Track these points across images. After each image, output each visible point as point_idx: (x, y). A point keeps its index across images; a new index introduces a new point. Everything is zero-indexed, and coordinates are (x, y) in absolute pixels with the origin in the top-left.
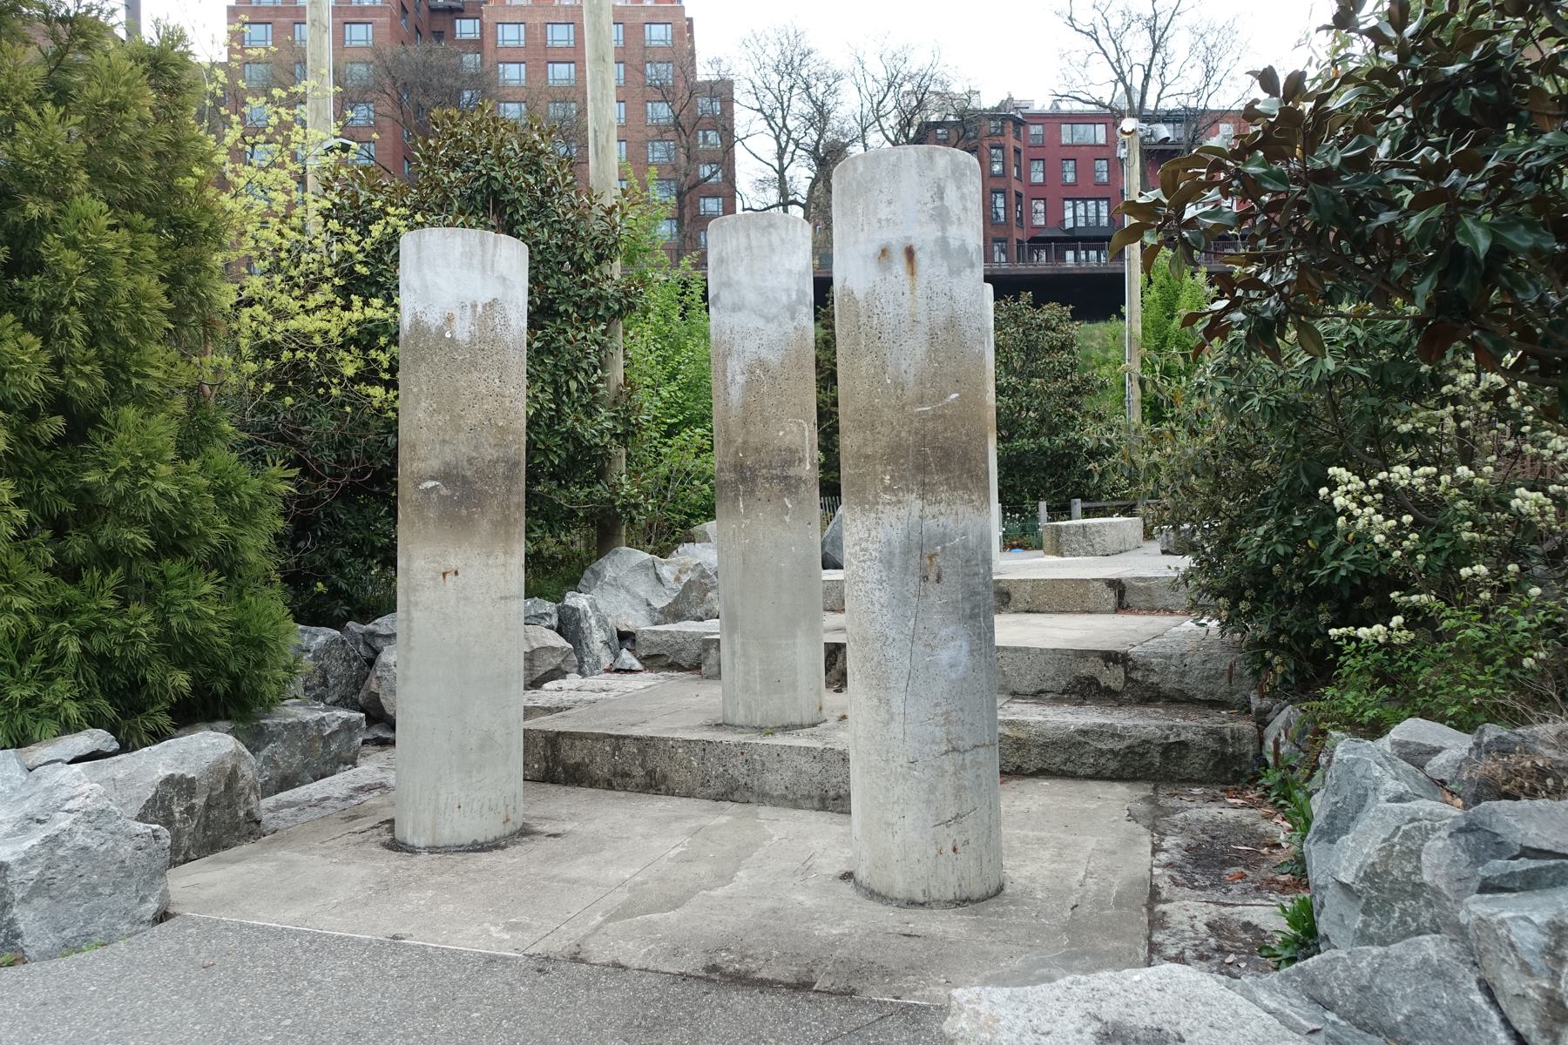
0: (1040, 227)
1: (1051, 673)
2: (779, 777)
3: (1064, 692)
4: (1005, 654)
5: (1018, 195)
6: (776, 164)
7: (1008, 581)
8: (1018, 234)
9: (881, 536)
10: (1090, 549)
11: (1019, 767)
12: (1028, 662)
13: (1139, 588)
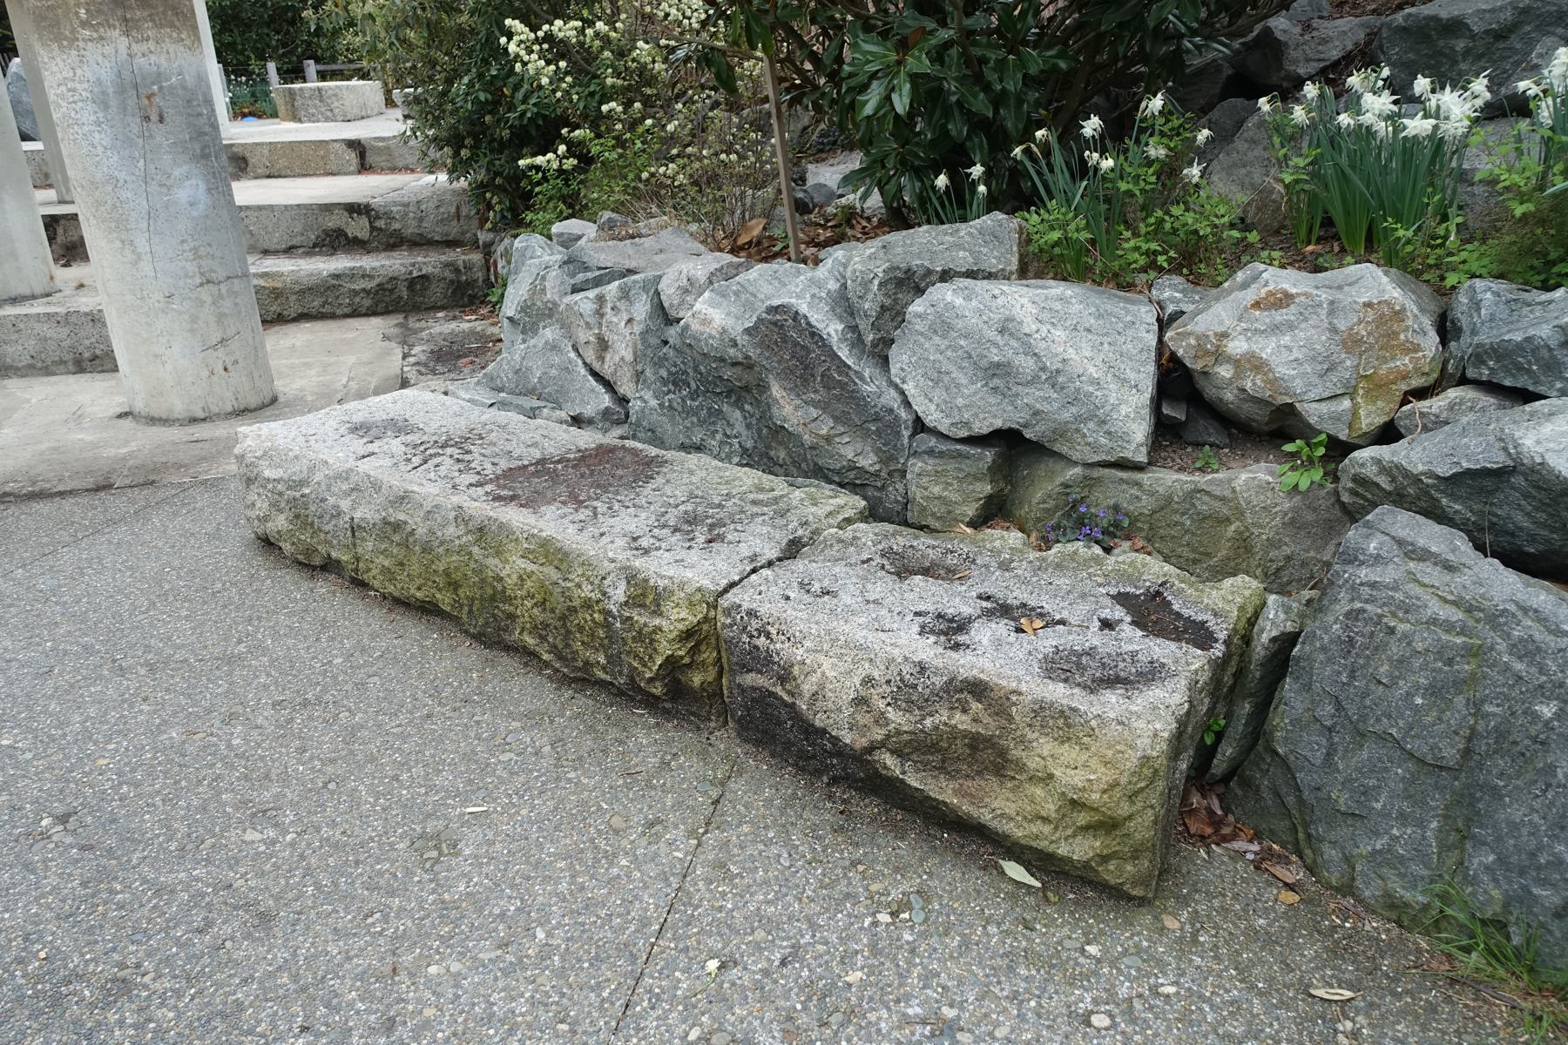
1: (299, 228)
2: (20, 348)
3: (315, 245)
4: (248, 213)
7: (242, 145)
9: (89, 74)
10: (329, 114)
11: (280, 314)
12: (275, 220)
13: (379, 148)
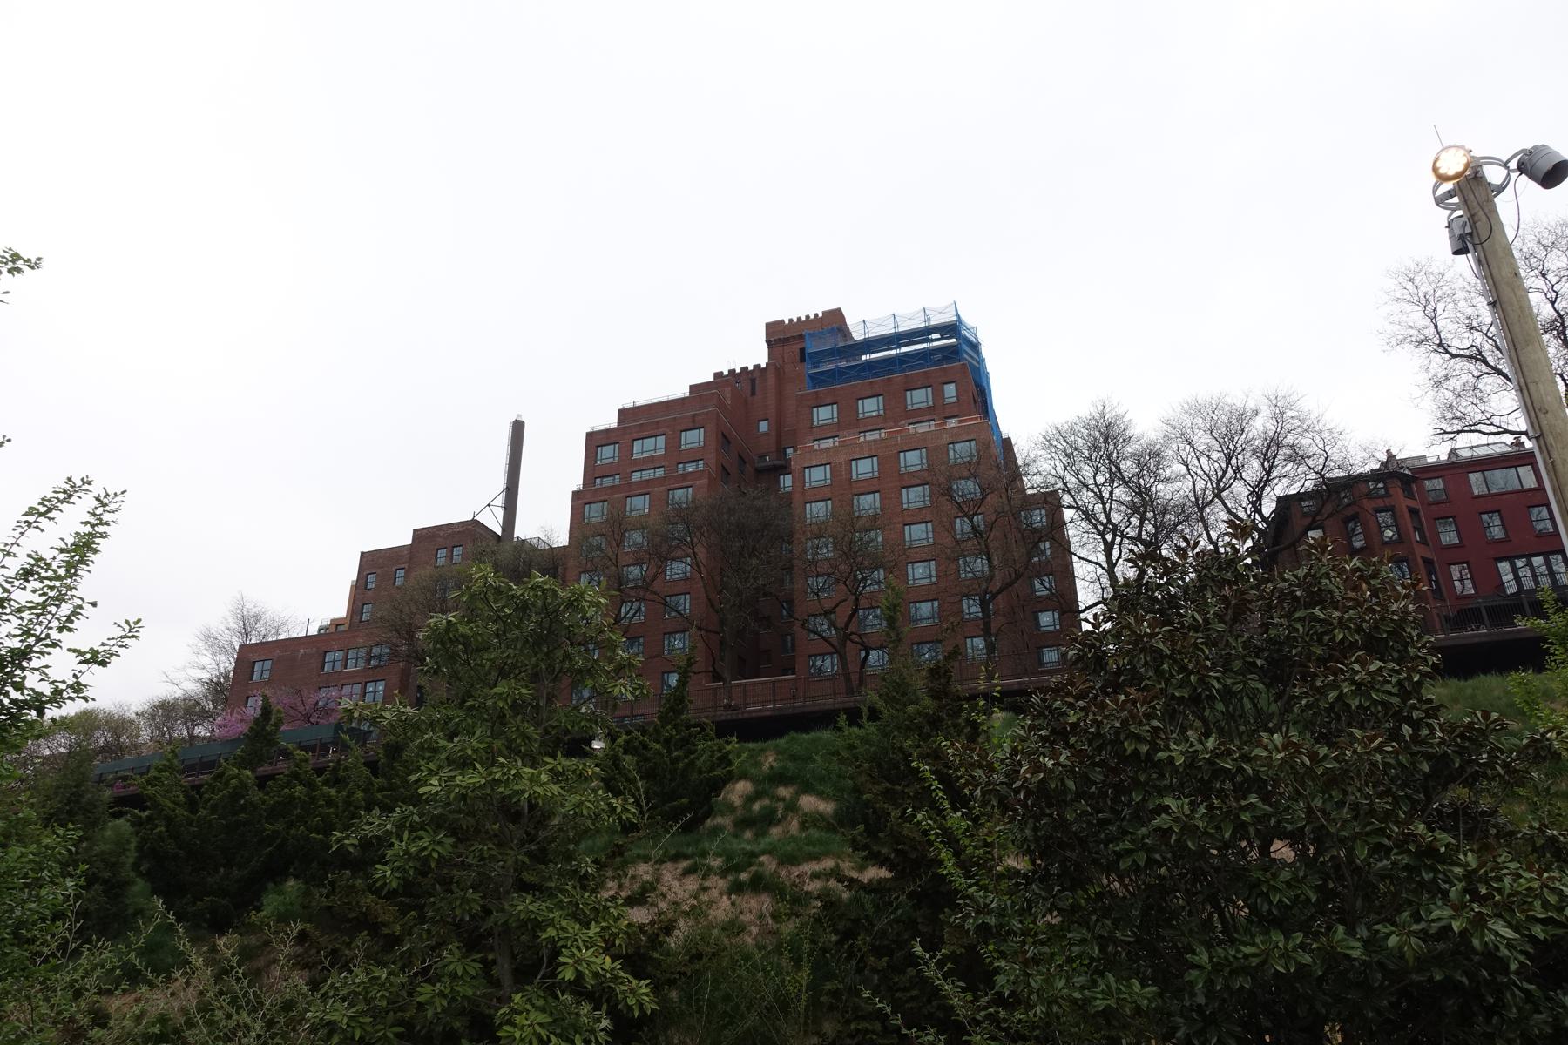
6: (1102, 559)
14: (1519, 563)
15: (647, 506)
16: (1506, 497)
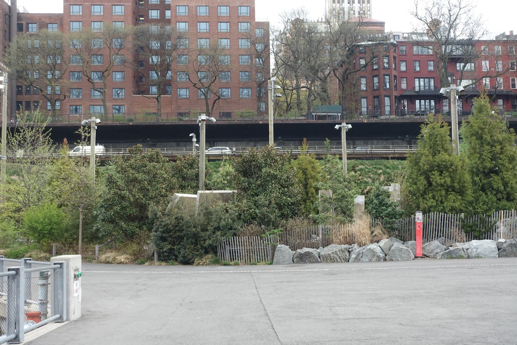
0: (404, 90)
5: (395, 76)
8: (395, 93)
14: (421, 80)
15: (102, 11)
16: (423, 56)
